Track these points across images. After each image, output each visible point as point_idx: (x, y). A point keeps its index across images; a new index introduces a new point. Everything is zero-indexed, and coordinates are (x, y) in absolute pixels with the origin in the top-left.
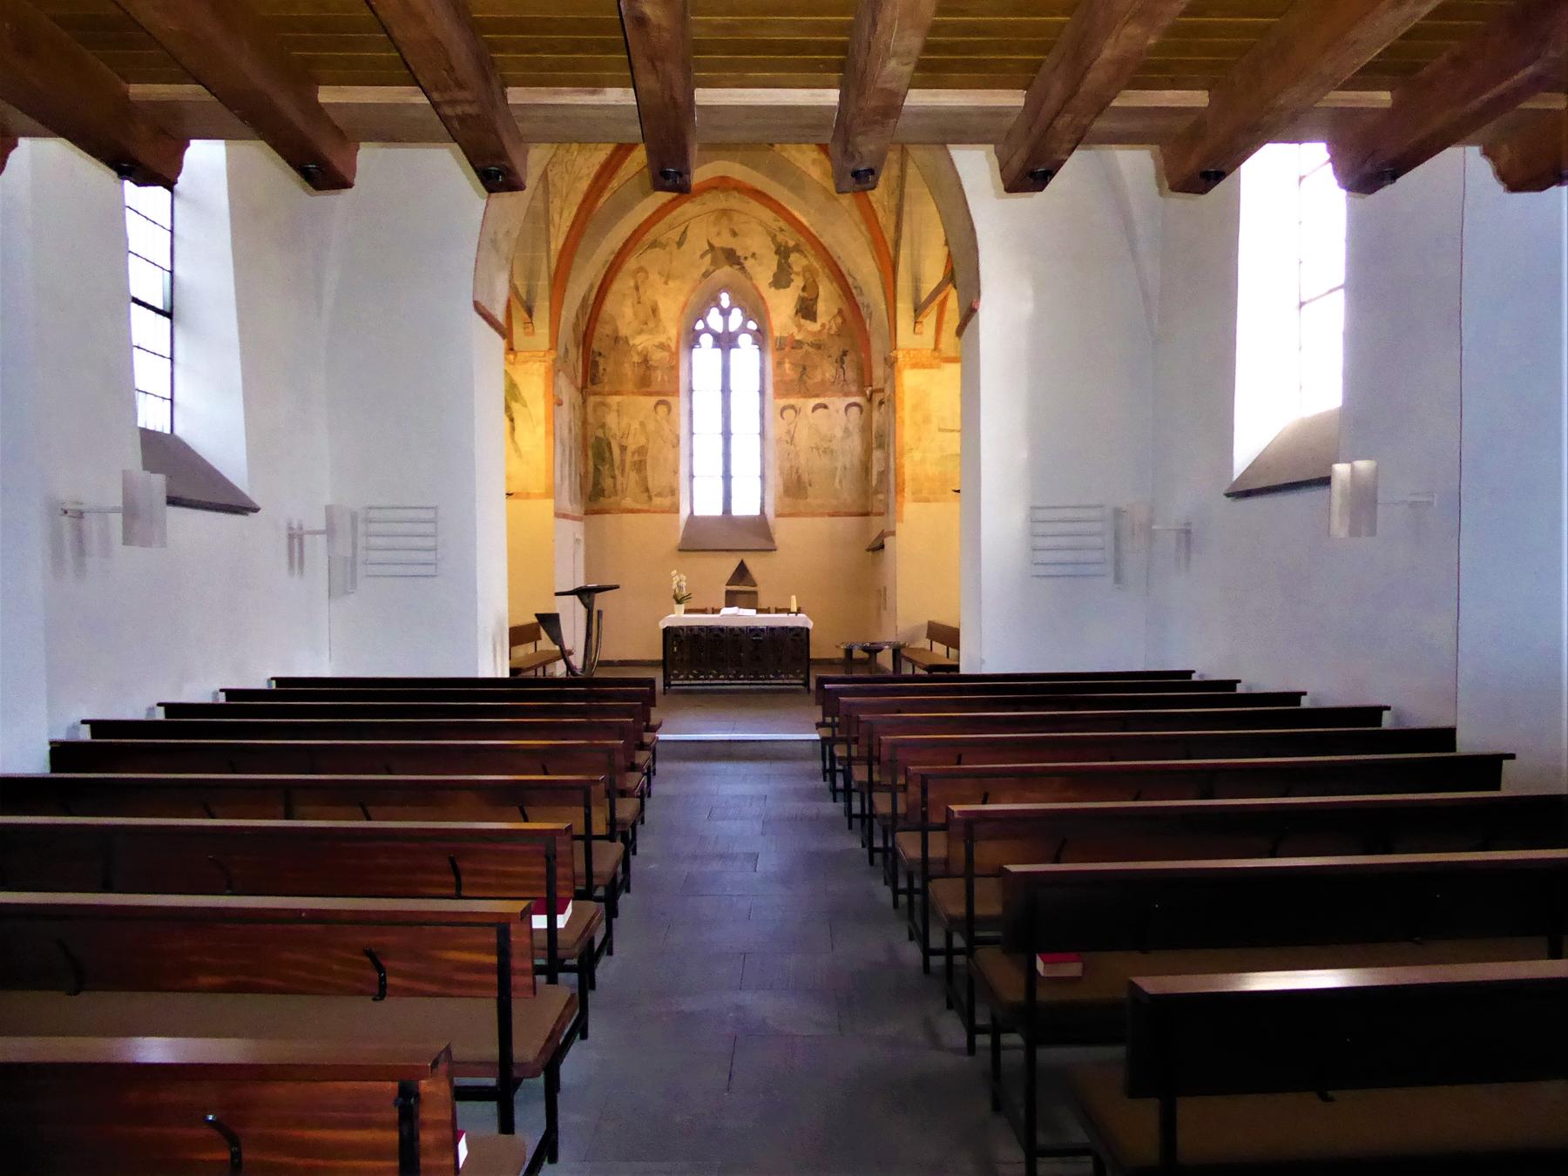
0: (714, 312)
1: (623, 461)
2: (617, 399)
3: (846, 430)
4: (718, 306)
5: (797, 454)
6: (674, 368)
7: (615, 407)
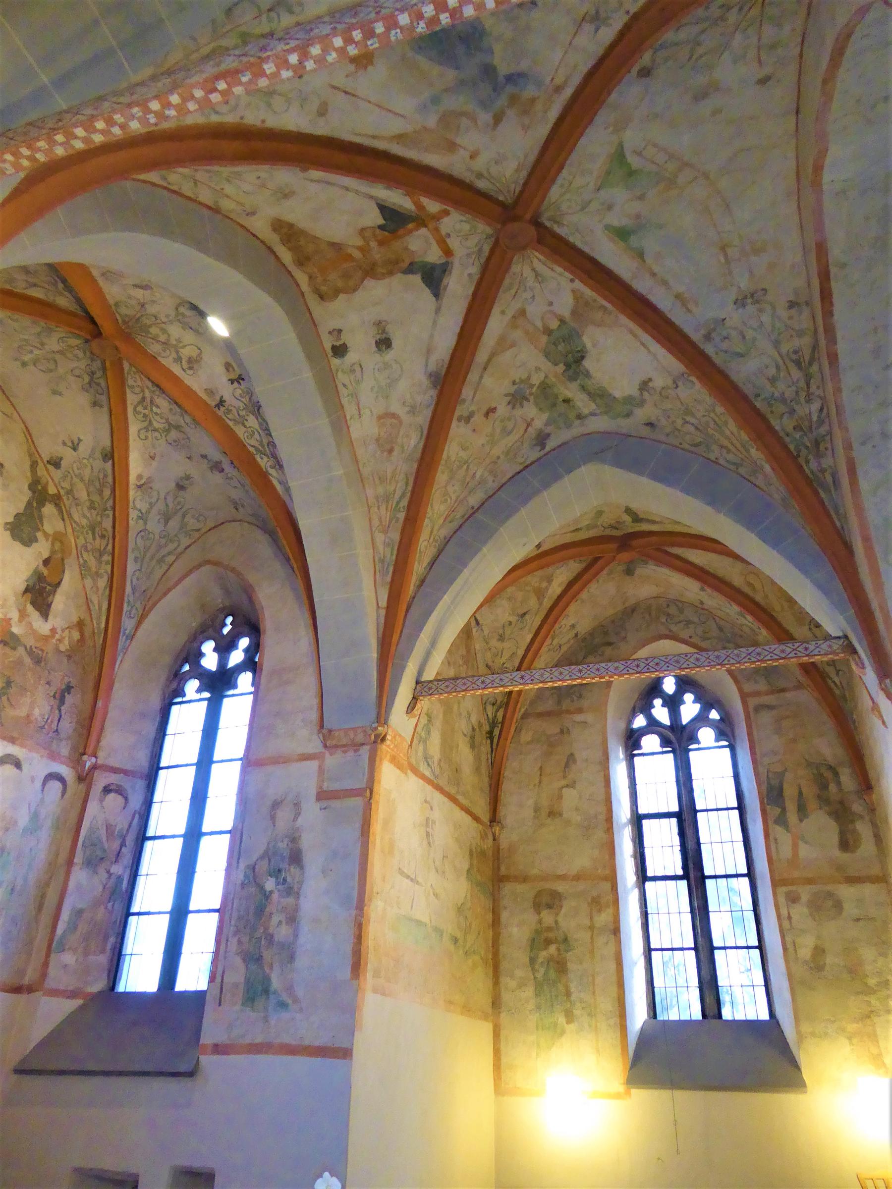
3: (35, 816)
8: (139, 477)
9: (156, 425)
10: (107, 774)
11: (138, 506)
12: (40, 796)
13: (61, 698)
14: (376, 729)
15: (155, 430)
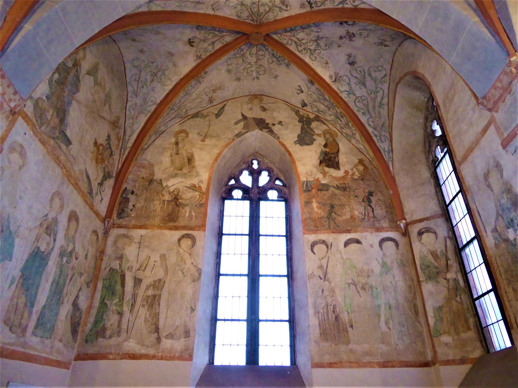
0: (246, 173)
1: (134, 296)
2: (143, 232)
3: (384, 265)
5: (332, 291)
6: (203, 206)
7: (137, 240)
8: (331, 77)
9: (312, 48)
10: (416, 225)
11: (343, 90)
12: (381, 253)
13: (368, 199)
14: (510, 62)
15: (315, 50)
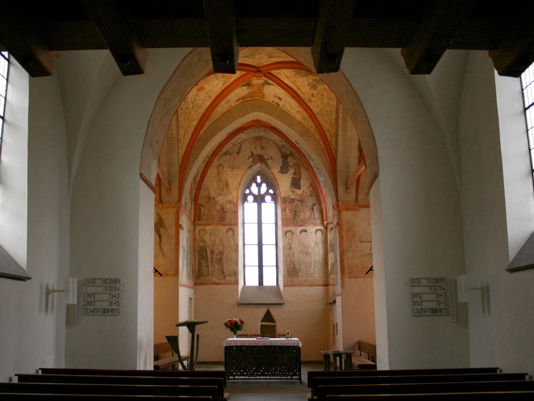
4: (256, 182)
6: (236, 212)
